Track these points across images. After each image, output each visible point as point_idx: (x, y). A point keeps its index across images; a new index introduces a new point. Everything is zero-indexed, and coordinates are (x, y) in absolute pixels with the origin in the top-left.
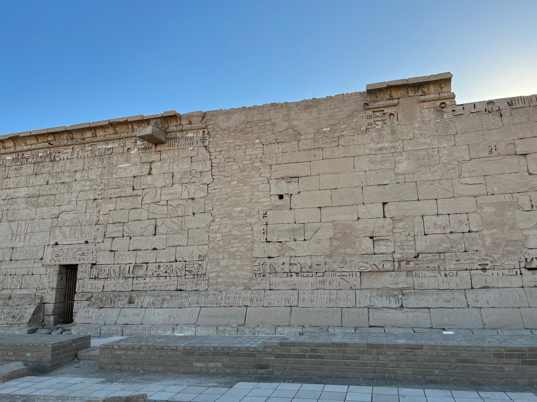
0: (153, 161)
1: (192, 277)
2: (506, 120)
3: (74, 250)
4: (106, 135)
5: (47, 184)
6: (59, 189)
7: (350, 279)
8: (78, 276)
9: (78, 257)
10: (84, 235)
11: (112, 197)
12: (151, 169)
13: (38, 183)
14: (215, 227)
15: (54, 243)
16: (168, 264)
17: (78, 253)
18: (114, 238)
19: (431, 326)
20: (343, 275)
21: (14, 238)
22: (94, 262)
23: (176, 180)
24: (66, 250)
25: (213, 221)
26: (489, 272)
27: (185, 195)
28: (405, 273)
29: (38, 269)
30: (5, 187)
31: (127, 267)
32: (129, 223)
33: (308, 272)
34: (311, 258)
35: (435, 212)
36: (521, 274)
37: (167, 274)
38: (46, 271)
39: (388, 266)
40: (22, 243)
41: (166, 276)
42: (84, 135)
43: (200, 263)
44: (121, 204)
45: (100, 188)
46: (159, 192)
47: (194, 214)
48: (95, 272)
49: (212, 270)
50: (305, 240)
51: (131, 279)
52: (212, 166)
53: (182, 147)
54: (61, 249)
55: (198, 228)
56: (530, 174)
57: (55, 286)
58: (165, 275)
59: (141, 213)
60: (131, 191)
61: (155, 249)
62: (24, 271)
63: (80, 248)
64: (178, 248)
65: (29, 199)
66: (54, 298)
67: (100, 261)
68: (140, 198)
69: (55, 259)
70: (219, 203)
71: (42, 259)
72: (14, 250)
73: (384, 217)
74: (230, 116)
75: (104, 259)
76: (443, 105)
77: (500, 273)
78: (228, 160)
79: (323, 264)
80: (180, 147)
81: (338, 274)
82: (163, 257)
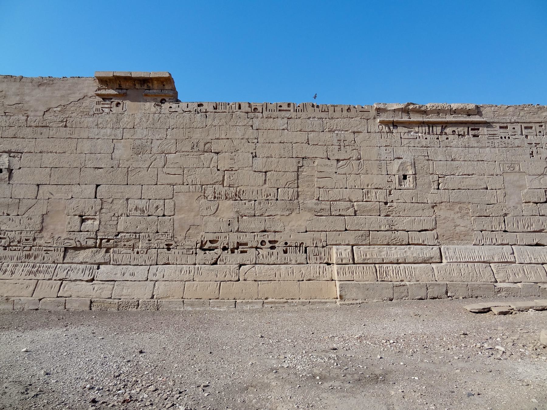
2: (209, 122)
7: (56, 253)
19: (110, 296)
20: (49, 251)
26: (173, 251)
28: (105, 249)
33: (16, 246)
34: (21, 233)
35: (139, 197)
36: (196, 253)
39: (91, 242)
50: (18, 215)
56: (218, 170)
73: (96, 198)
76: (163, 101)
77: (181, 251)
79: (31, 239)
81: (45, 248)
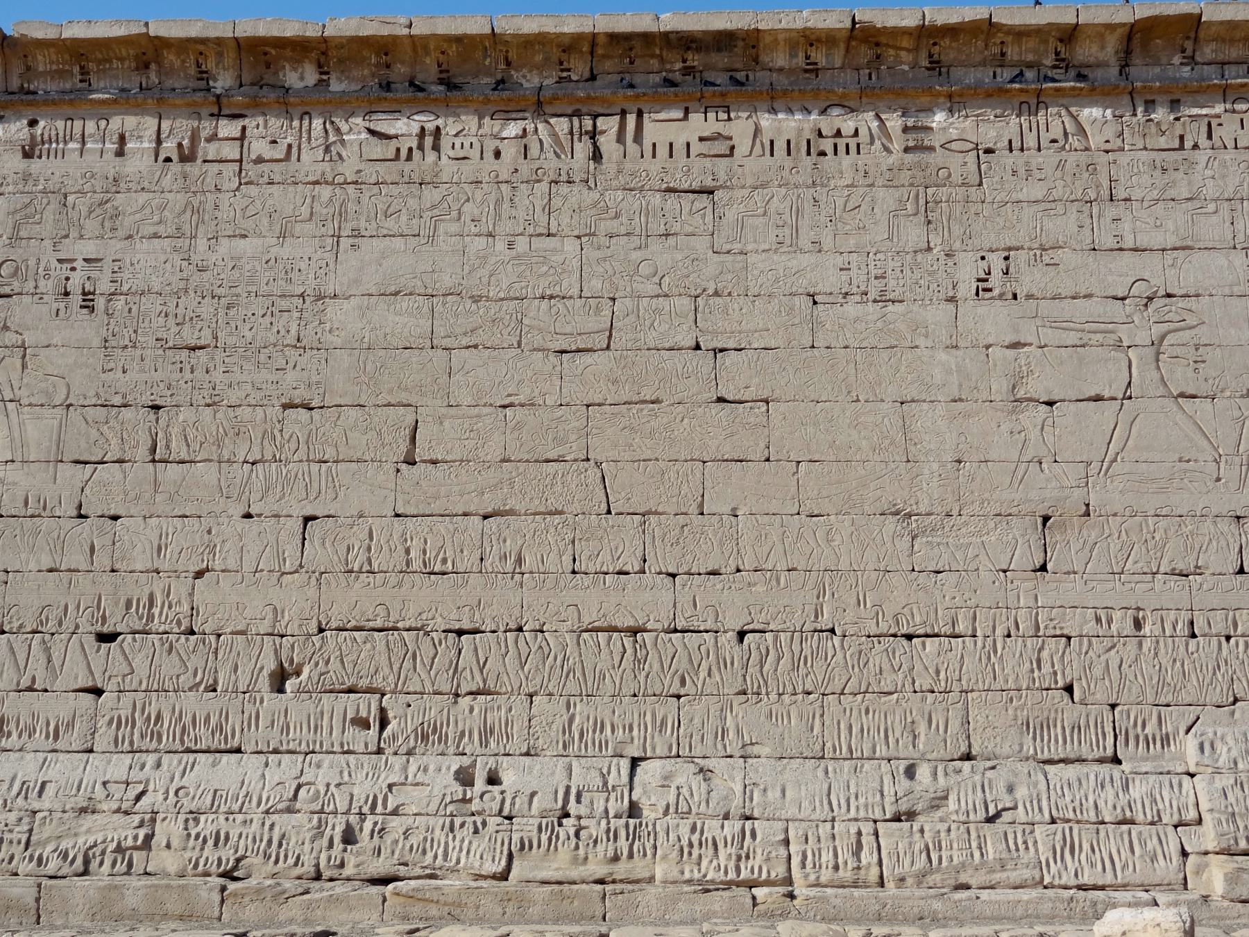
30: (1111, 242)
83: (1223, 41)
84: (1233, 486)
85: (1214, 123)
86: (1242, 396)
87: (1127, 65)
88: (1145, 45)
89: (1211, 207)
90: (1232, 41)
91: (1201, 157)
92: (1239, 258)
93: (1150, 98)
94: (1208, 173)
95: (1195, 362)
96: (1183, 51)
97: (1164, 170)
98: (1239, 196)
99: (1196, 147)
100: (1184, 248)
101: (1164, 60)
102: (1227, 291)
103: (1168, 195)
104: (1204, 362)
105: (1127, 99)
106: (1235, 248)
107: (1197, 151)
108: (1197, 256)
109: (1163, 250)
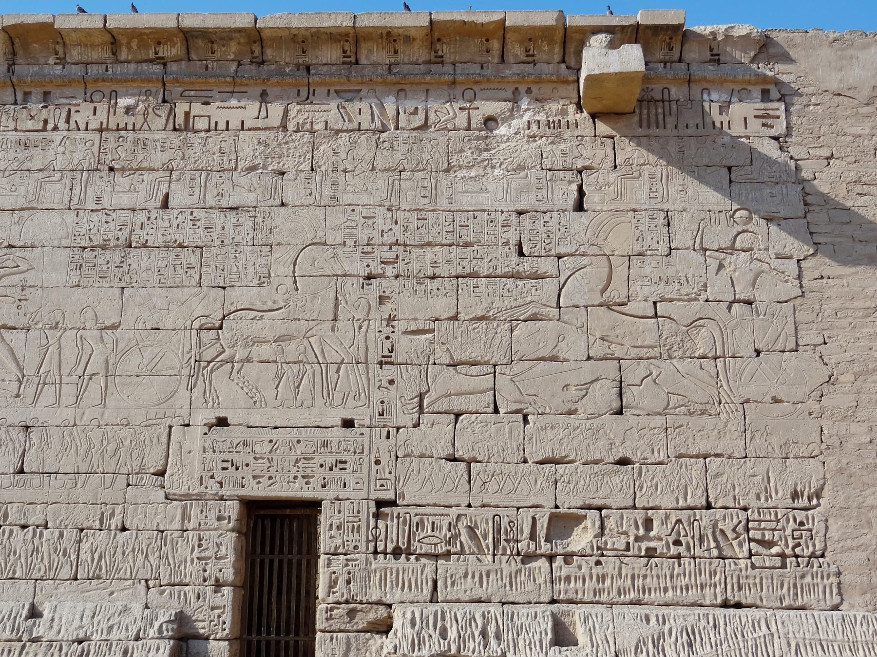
0: (586, 168)
1: (778, 561)
3: (300, 449)
4: (397, 64)
5: (165, 205)
6: (217, 230)
8: (324, 543)
9: (320, 473)
10: (338, 396)
11: (438, 271)
12: (581, 193)
13: (126, 202)
14: (838, 399)
15: (211, 416)
16: (684, 515)
17: (318, 460)
18: (457, 415)
21: (29, 392)
22: (389, 495)
23: (683, 237)
24: (267, 447)
25: (830, 380)
27: (718, 287)
29: (149, 509)
31: (526, 517)
32: (516, 368)
37: (682, 549)
38: (185, 517)
40: (67, 414)
41: (679, 557)
42: (310, 52)
43: (800, 516)
44: (474, 299)
45: (389, 238)
46: (620, 273)
47: (758, 353)
48: (391, 531)
49: (849, 543)
51: (543, 563)
52: (806, 204)
53: (690, 131)
54: (245, 444)
55: (776, 401)
57: (229, 574)
58: (674, 550)
59: (560, 337)
60: (514, 258)
61: (624, 462)
62: (87, 515)
63: (325, 444)
64: (714, 464)
65: (87, 253)
66: (227, 617)
67: (412, 492)
68: (549, 287)
69: (219, 475)
70: (845, 322)
71: (162, 473)
72: (34, 436)
74: (851, 52)
75: (425, 486)
78: (858, 189)
80: (683, 131)
82: (662, 490)
83: (86, 45)
84: (29, 400)
85: (73, 109)
86: (51, 328)
87: (14, 64)
88: (26, 47)
89: (58, 176)
90: (92, 46)
91: (57, 136)
92: (70, 217)
93: (27, 90)
94: (61, 149)
95: (19, 300)
96: (57, 54)
97: (26, 147)
98: (80, 167)
99: (55, 128)
100: (28, 209)
101: (42, 60)
102: (56, 243)
103: (25, 167)
104: (26, 300)
105: (10, 90)
106: (69, 209)
107: (55, 132)
108: (38, 215)
109: (13, 210)
